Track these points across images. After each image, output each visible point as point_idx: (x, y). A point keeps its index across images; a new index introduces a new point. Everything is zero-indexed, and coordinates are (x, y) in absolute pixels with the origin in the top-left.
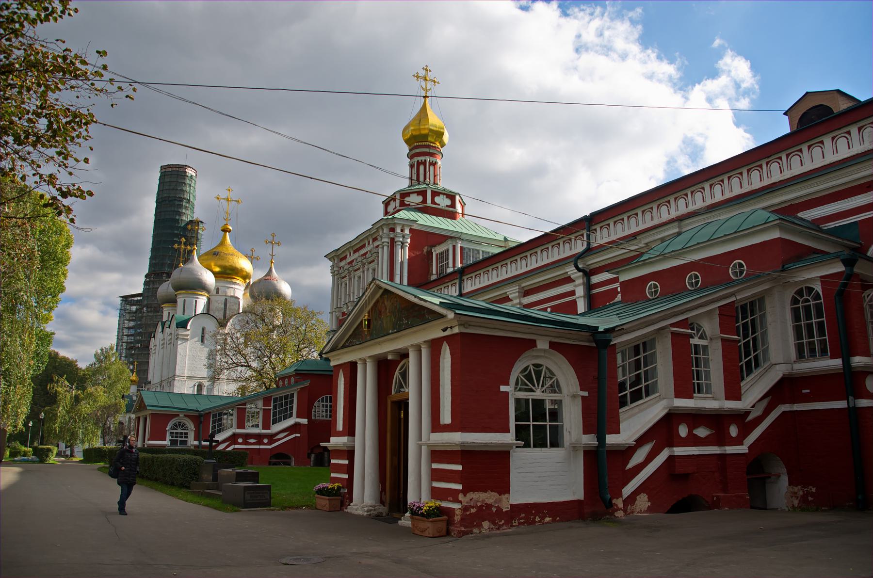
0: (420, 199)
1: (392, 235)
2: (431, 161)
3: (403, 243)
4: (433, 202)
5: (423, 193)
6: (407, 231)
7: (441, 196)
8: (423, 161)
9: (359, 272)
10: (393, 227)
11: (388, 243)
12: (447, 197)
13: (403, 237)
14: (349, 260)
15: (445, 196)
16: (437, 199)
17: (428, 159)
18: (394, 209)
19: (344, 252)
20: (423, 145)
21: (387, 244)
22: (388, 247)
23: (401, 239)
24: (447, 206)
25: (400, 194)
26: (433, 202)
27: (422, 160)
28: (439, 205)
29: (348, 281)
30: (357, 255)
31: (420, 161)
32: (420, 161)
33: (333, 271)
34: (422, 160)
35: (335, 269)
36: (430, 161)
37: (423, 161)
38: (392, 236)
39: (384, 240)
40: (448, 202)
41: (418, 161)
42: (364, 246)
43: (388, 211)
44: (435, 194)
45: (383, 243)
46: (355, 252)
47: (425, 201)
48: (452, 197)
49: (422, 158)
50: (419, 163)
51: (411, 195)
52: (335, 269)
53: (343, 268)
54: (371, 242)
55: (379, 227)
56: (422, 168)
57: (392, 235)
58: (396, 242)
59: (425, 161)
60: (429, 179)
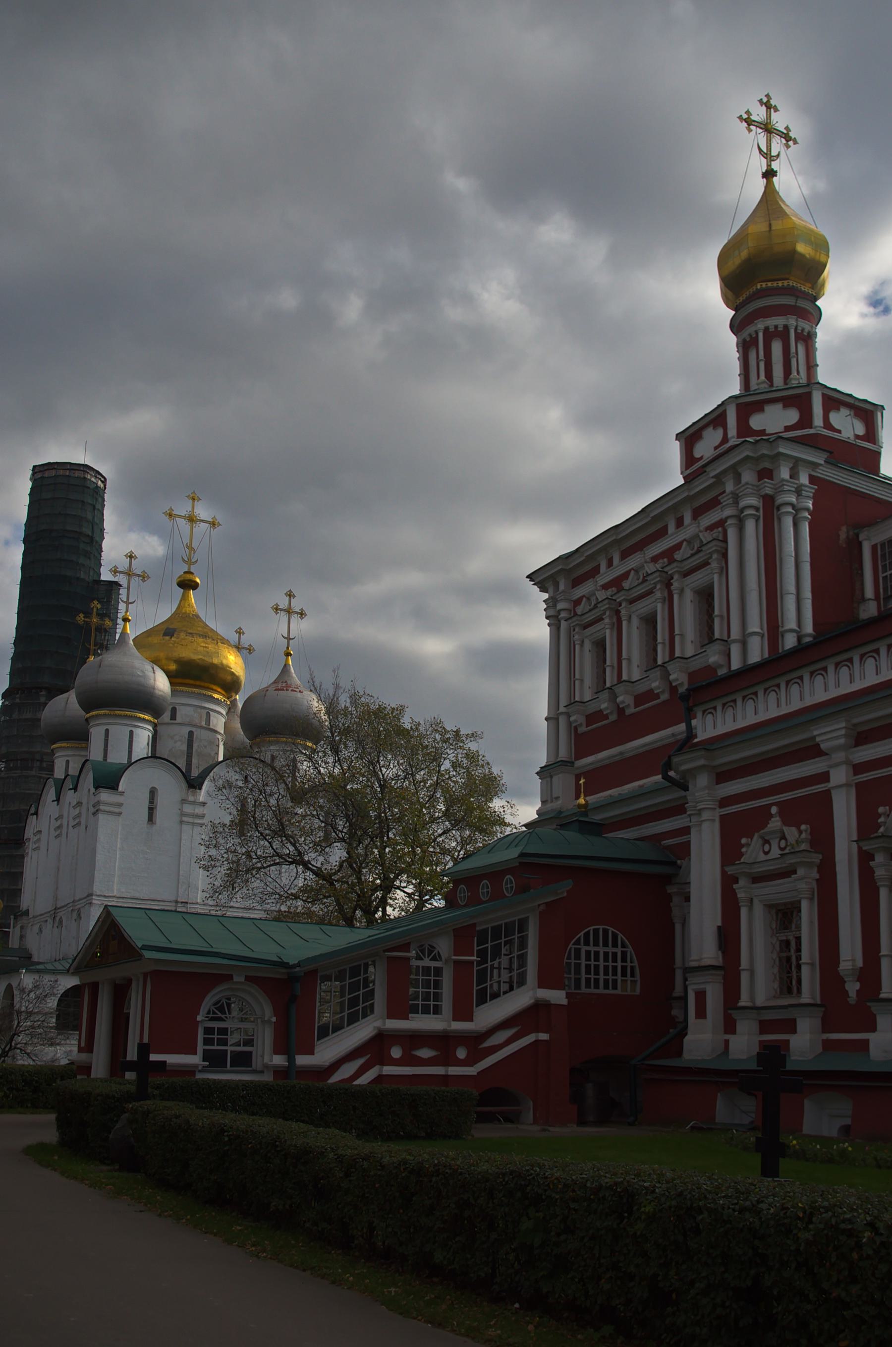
0: (792, 416)
2: (799, 328)
3: (797, 509)
4: (828, 425)
6: (804, 479)
7: (844, 411)
8: (780, 329)
9: (653, 599)
10: (767, 465)
11: (757, 509)
13: (798, 492)
14: (604, 576)
17: (792, 321)
18: (716, 448)
19: (591, 557)
20: (778, 288)
21: (753, 512)
22: (757, 521)
23: (793, 499)
24: (857, 437)
25: (738, 405)
28: (839, 432)
31: (772, 329)
32: (772, 329)
33: (552, 612)
34: (776, 327)
35: (560, 606)
37: (780, 329)
38: (768, 491)
40: (860, 429)
41: (766, 329)
42: (662, 533)
43: (697, 454)
45: (742, 511)
46: (625, 555)
47: (806, 420)
49: (779, 321)
50: (769, 335)
51: (769, 409)
52: (560, 606)
53: (588, 599)
54: (688, 519)
55: (724, 472)
56: (777, 348)
58: (778, 509)
59: (786, 327)
60: (798, 373)
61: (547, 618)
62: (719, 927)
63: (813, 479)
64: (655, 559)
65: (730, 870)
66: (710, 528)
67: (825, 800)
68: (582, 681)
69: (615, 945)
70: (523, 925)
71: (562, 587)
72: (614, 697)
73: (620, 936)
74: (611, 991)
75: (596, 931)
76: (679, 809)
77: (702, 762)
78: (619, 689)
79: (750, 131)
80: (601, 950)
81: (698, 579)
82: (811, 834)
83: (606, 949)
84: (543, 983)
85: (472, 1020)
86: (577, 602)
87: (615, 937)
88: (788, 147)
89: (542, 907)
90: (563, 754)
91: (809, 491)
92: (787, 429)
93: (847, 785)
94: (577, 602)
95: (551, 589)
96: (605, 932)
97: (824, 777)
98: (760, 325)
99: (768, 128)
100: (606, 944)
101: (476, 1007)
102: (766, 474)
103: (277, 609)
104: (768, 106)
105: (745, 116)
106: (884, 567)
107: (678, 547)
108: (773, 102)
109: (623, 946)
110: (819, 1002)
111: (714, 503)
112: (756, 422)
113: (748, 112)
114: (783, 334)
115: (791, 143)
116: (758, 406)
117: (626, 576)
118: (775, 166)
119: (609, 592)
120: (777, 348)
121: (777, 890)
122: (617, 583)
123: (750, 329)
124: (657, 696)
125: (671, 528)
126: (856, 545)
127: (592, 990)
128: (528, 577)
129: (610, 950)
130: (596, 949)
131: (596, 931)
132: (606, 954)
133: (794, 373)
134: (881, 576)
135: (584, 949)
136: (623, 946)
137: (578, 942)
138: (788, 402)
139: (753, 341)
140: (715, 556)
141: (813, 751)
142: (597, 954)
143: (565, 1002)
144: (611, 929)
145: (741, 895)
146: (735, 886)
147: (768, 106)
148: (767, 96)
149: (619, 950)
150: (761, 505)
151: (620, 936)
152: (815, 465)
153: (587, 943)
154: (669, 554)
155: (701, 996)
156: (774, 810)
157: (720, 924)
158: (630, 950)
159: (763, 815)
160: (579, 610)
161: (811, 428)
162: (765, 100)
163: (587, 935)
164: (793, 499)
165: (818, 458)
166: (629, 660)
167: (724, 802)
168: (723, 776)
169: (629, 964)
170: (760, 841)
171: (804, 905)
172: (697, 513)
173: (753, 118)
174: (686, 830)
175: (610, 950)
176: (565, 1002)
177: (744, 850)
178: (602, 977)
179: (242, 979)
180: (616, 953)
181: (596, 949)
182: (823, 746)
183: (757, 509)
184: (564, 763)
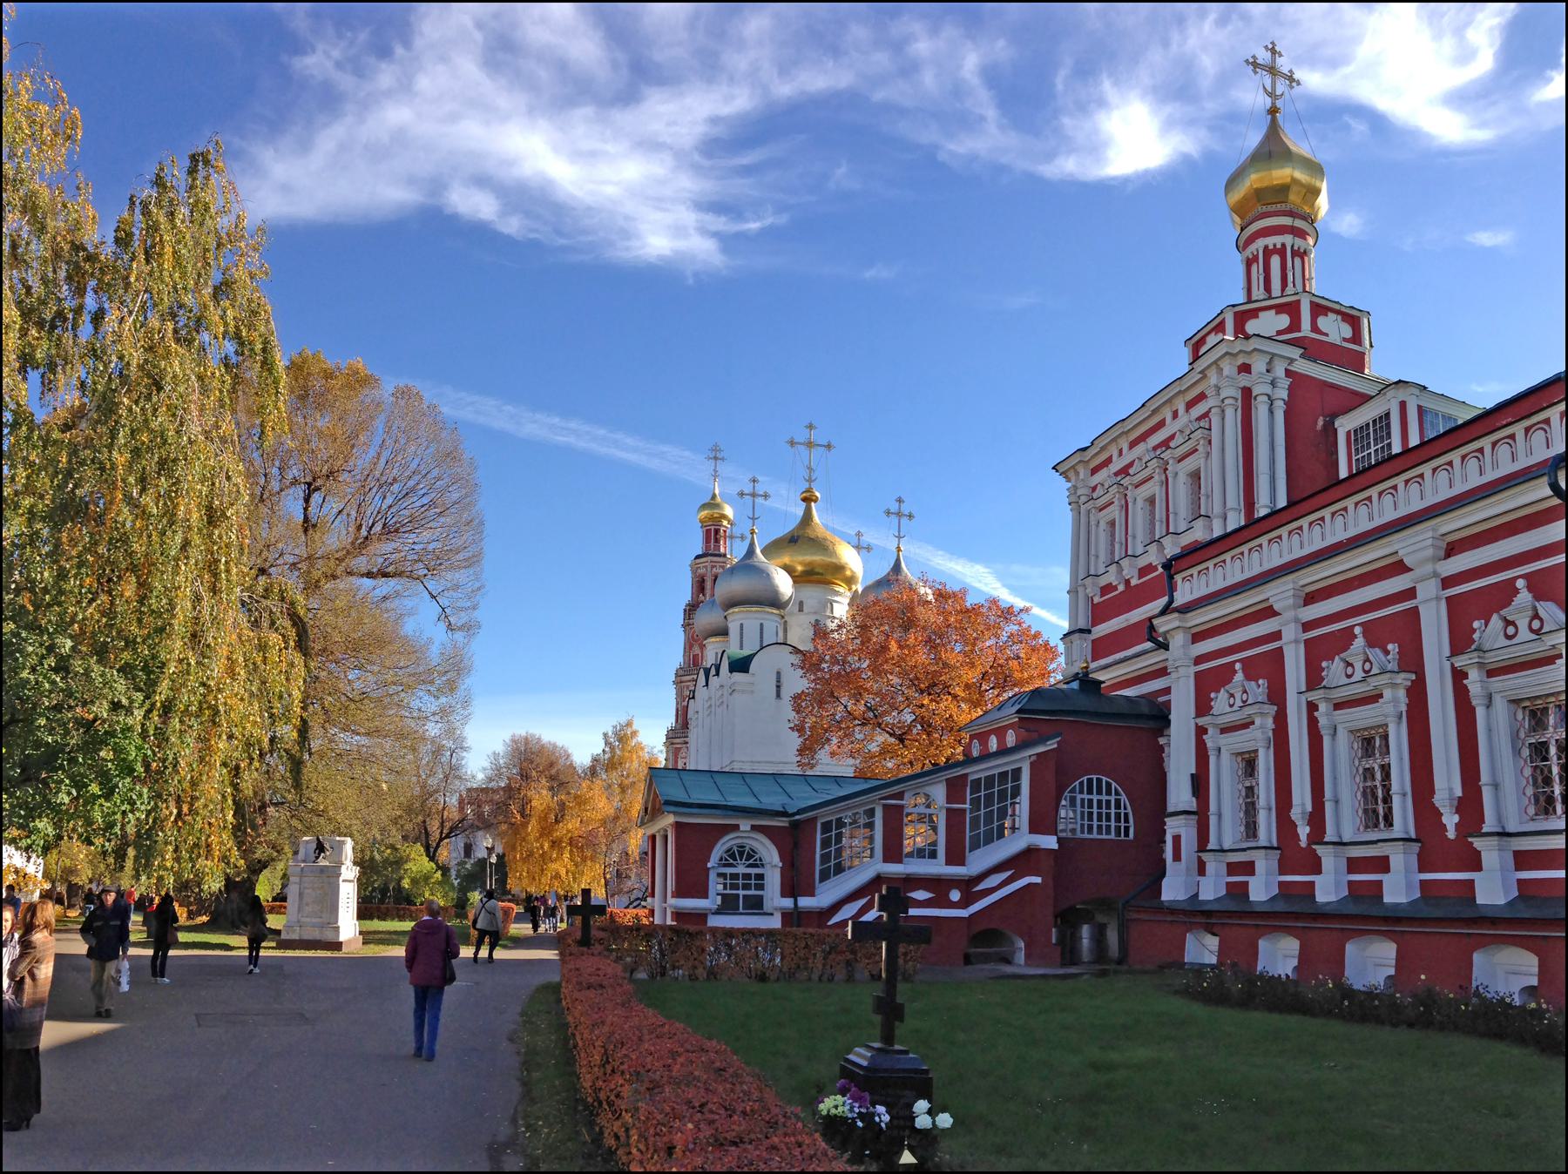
0: (1284, 321)
1: (1244, 380)
2: (1296, 248)
3: (1271, 401)
4: (1315, 329)
5: (1292, 309)
6: (1279, 371)
7: (1332, 316)
8: (1279, 246)
11: (1236, 399)
12: (1343, 320)
13: (1273, 384)
14: (1117, 465)
15: (1339, 317)
16: (1324, 322)
17: (1288, 239)
24: (1345, 340)
25: (1236, 314)
26: (1315, 329)
27: (1275, 245)
28: (1327, 335)
29: (1117, 512)
30: (1140, 449)
31: (1271, 247)
32: (1271, 247)
33: (1073, 499)
35: (1079, 493)
36: (1292, 246)
38: (1248, 384)
39: (1224, 394)
40: (1347, 331)
41: (1266, 247)
42: (1161, 424)
44: (1319, 309)
45: (1223, 401)
46: (1133, 445)
47: (1295, 325)
48: (1353, 319)
50: (1268, 253)
51: (1261, 314)
55: (1209, 366)
56: (1275, 261)
57: (1244, 380)
59: (1283, 245)
60: (1294, 286)
61: (1070, 504)
62: (1192, 775)
63: (1288, 373)
64: (1155, 448)
65: (1202, 721)
66: (1199, 419)
67: (1277, 659)
68: (1097, 557)
69: (1109, 793)
70: (1017, 773)
71: (1082, 476)
72: (1120, 570)
73: (1114, 784)
74: (1104, 837)
75: (1090, 781)
76: (1162, 672)
77: (1177, 623)
78: (1125, 563)
79: (1256, 73)
80: (1095, 798)
81: (1190, 464)
82: (1268, 687)
83: (1100, 797)
84: (1034, 829)
85: (963, 864)
86: (1094, 489)
87: (1109, 785)
88: (1292, 87)
89: (1033, 758)
90: (1082, 624)
91: (1285, 383)
92: (1279, 333)
93: (1296, 641)
94: (1094, 489)
95: (1073, 479)
96: (1099, 781)
97: (1277, 636)
98: (1260, 243)
99: (1272, 70)
100: (1099, 792)
101: (970, 851)
102: (1245, 368)
103: (889, 513)
104: (1273, 51)
105: (1251, 60)
106: (1357, 450)
107: (1172, 437)
108: (1277, 49)
109: (1117, 793)
110: (1275, 844)
111: (1202, 397)
112: (1252, 327)
113: (1254, 57)
114: (1281, 252)
115: (1294, 84)
116: (1254, 313)
117: (1131, 464)
118: (1279, 104)
119: (1119, 478)
120: (1275, 261)
121: (1240, 740)
122: (1124, 471)
123: (1252, 248)
124: (1155, 569)
125: (1169, 420)
126: (1330, 431)
127: (1086, 836)
128: (1054, 468)
129: (1104, 798)
130: (1090, 797)
131: (1090, 781)
132: (1099, 802)
133: (1290, 285)
134: (1354, 458)
135: (1079, 797)
136: (1117, 793)
137: (1073, 791)
138: (1280, 309)
139: (1256, 258)
140: (1202, 442)
141: (1269, 612)
142: (1091, 801)
143: (1055, 846)
144: (1104, 779)
145: (1209, 744)
146: (1204, 737)
147: (1273, 51)
148: (1273, 43)
149: (1112, 798)
150: (1239, 397)
151: (1114, 784)
152: (1292, 361)
153: (1081, 792)
154: (1165, 444)
155: (1177, 839)
156: (1238, 666)
157: (1194, 772)
158: (1123, 797)
159: (1228, 670)
160: (1095, 496)
161: (1300, 331)
162: (1270, 46)
163: (1081, 784)
164: (1268, 389)
165: (1295, 353)
166: (1134, 537)
167: (1199, 660)
168: (1197, 637)
169: (1122, 811)
170: (1226, 695)
171: (1261, 753)
172: (1190, 405)
173: (1258, 61)
174: (1167, 691)
175: (1104, 798)
176: (1055, 846)
177: (1212, 703)
178: (1095, 823)
179: (748, 828)
180: (1092, 800)
181: (1090, 797)
182: (1276, 607)
183: (1236, 399)
184: (1081, 631)
